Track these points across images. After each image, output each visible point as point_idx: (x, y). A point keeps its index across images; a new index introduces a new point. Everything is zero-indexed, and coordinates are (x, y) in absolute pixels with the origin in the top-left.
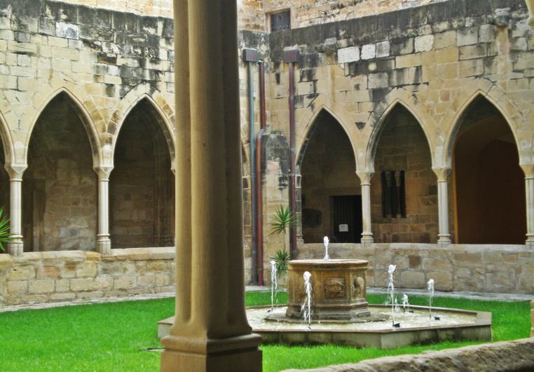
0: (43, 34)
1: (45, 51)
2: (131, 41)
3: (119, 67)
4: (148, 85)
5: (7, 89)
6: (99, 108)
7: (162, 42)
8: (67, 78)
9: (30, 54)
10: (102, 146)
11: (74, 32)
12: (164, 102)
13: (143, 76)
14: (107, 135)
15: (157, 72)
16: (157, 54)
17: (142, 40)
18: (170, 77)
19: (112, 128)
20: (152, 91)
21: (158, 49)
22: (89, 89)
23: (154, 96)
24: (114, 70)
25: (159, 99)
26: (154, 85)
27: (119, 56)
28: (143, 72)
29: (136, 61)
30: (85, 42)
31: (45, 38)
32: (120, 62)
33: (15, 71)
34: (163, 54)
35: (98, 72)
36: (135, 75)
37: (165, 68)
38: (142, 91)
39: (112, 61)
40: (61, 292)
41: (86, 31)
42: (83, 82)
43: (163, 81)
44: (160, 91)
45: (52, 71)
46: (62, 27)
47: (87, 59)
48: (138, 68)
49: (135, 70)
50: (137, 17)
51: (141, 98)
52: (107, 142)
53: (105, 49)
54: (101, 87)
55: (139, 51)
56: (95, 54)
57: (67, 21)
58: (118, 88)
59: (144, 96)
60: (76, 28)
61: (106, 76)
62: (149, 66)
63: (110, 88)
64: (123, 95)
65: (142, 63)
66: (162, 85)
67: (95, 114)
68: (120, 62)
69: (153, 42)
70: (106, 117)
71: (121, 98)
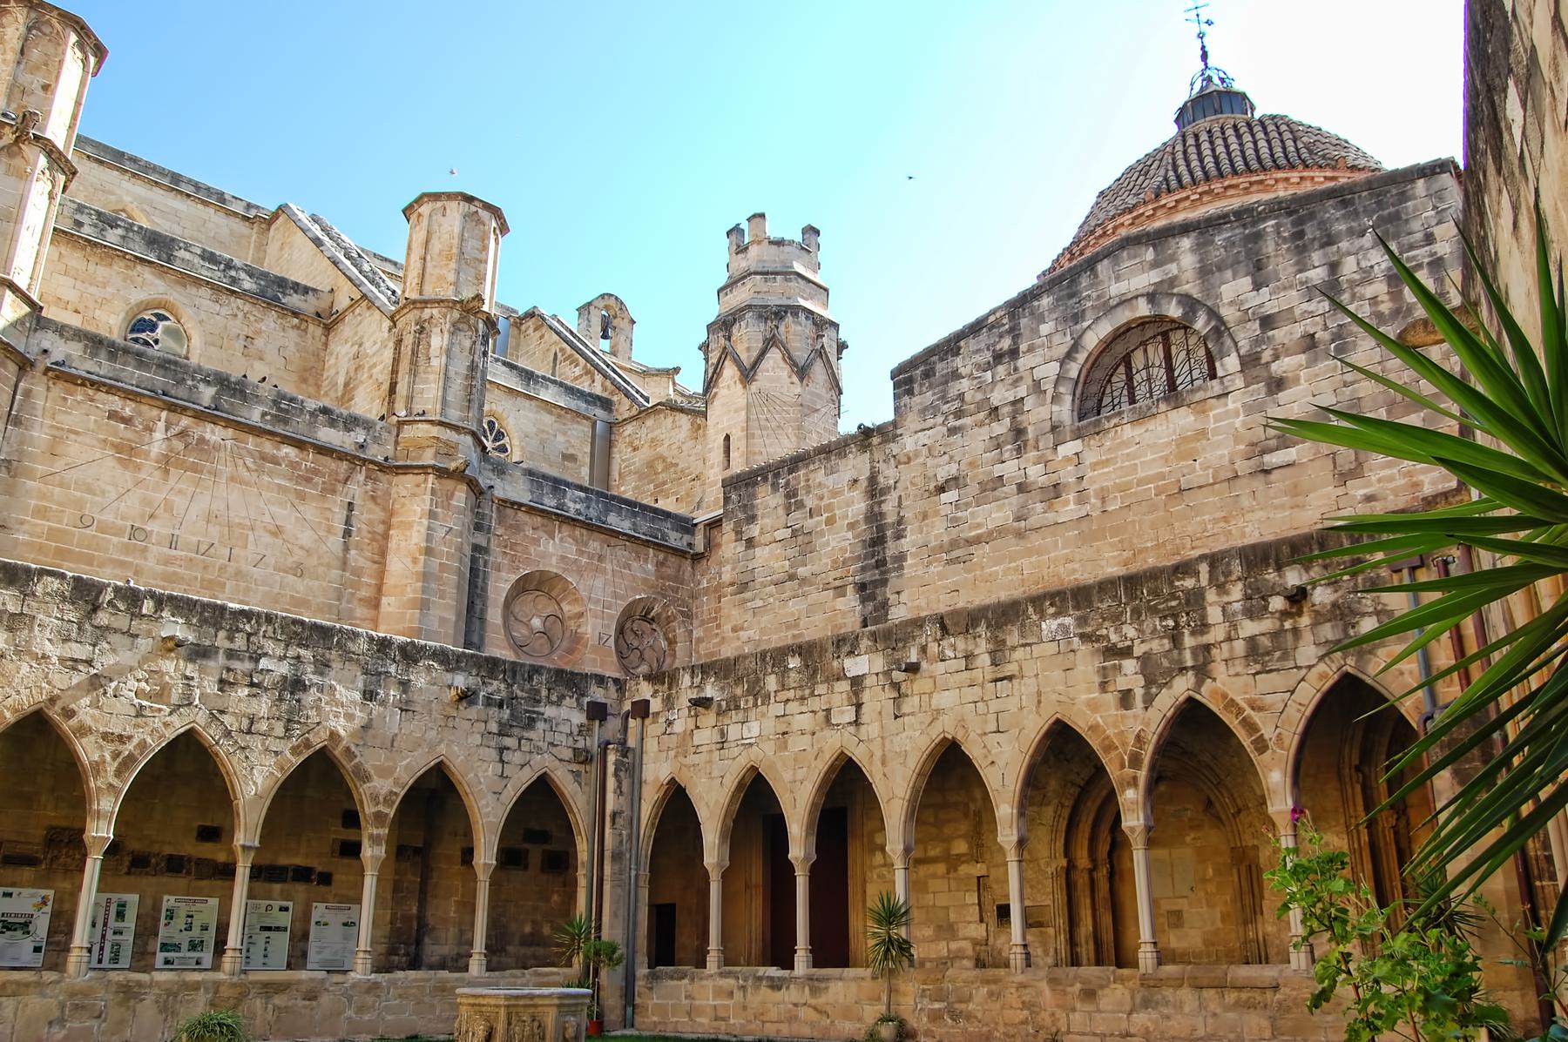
0: (1024, 645)
1: (1029, 669)
2: (1153, 610)
3: (1138, 658)
4: (1190, 673)
5: (985, 734)
6: (1110, 732)
7: (1211, 596)
8: (1062, 698)
9: (1010, 678)
10: (1123, 791)
11: (1064, 629)
12: (1225, 696)
13: (1180, 661)
14: (1129, 771)
15: (1207, 648)
16: (1203, 617)
17: (1174, 603)
18: (1231, 649)
19: (1135, 761)
20: (1199, 684)
21: (1204, 608)
22: (1093, 706)
23: (1203, 690)
24: (1130, 665)
25: (1214, 692)
26: (1202, 671)
27: (1136, 642)
28: (1180, 654)
29: (1166, 641)
30: (1084, 637)
31: (1028, 648)
32: (1139, 650)
33: (994, 706)
34: (1214, 614)
35: (1105, 676)
36: (1166, 663)
37: (1221, 637)
38: (1182, 687)
39: (1127, 652)
40: (1078, 1034)
41: (1082, 621)
42: (1084, 697)
43: (1218, 659)
44: (1214, 680)
45: (1039, 694)
46: (1049, 626)
47: (1087, 663)
48: (1170, 650)
49: (1165, 657)
50: (1162, 570)
51: (1182, 699)
52: (1129, 784)
53: (1114, 638)
54: (1111, 698)
55: (1171, 623)
56: (1098, 650)
57: (1055, 616)
58: (1139, 693)
59: (1186, 694)
60: (1068, 621)
61: (1120, 680)
62: (1189, 641)
63: (1126, 699)
64: (1149, 701)
65: (1176, 640)
66: (1219, 669)
67: (1107, 742)
68: (1139, 650)
69: (1195, 600)
70: (1124, 744)
71: (1146, 708)
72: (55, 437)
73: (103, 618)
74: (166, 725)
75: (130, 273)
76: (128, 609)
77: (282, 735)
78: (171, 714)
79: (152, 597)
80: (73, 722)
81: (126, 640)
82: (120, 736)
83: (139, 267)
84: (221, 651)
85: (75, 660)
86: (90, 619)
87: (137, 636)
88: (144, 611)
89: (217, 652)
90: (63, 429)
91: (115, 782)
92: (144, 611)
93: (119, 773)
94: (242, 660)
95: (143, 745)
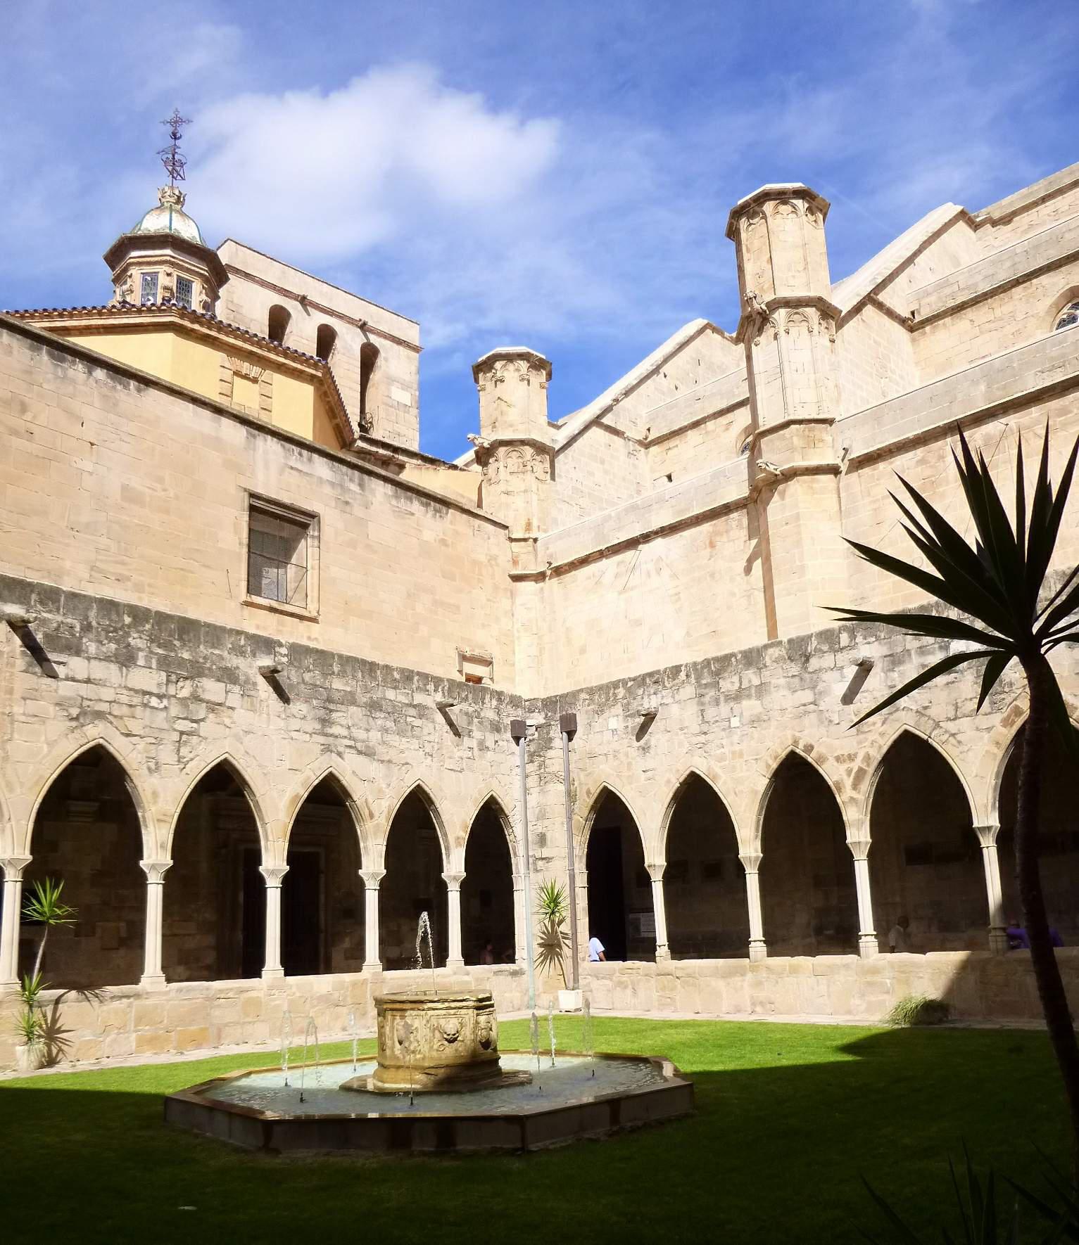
72: (875, 510)
73: (814, 663)
74: (882, 734)
75: (1030, 291)
76: (830, 648)
77: (989, 710)
78: (884, 723)
79: (844, 630)
80: (814, 754)
81: (836, 674)
82: (849, 755)
83: (1034, 281)
84: (913, 652)
85: (805, 705)
86: (806, 668)
87: (842, 667)
88: (842, 645)
89: (910, 655)
90: (878, 500)
91: (855, 794)
92: (842, 645)
93: (855, 786)
94: (933, 653)
95: (867, 758)
